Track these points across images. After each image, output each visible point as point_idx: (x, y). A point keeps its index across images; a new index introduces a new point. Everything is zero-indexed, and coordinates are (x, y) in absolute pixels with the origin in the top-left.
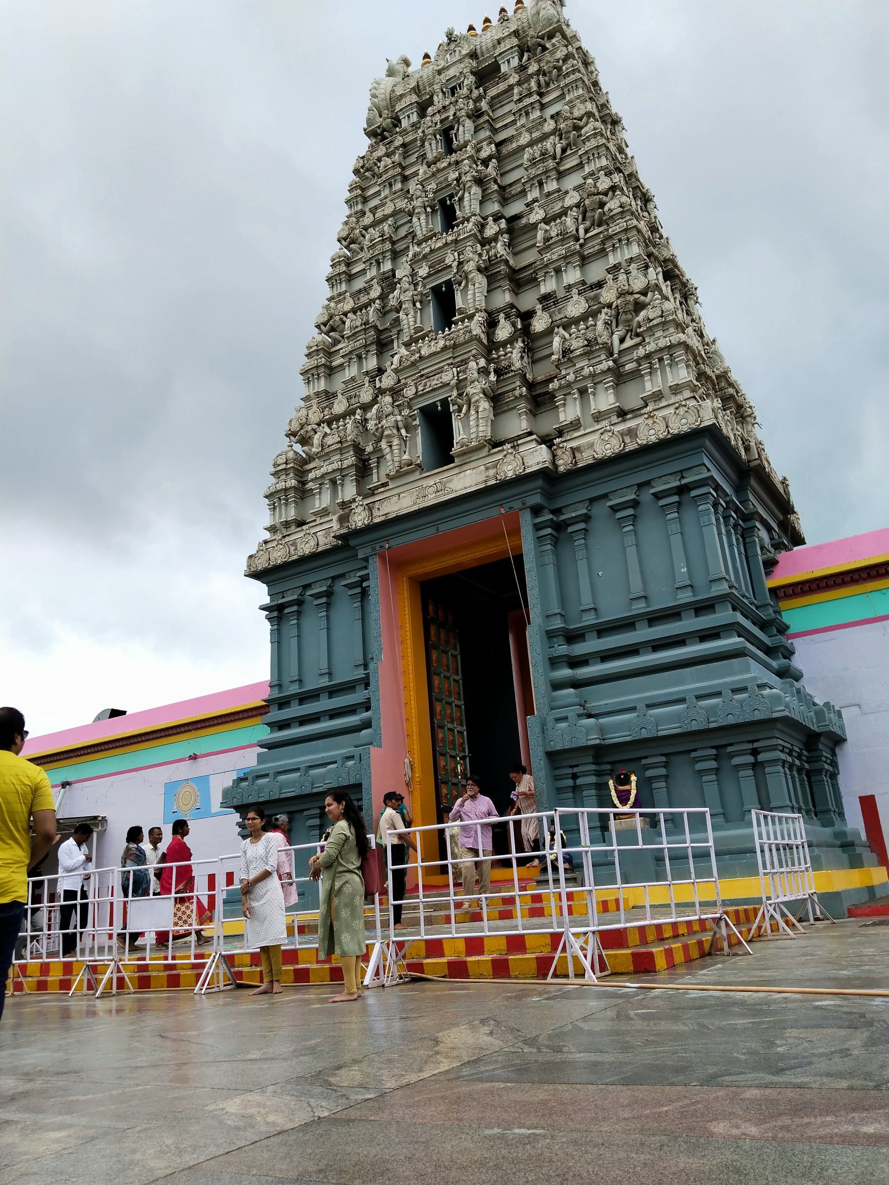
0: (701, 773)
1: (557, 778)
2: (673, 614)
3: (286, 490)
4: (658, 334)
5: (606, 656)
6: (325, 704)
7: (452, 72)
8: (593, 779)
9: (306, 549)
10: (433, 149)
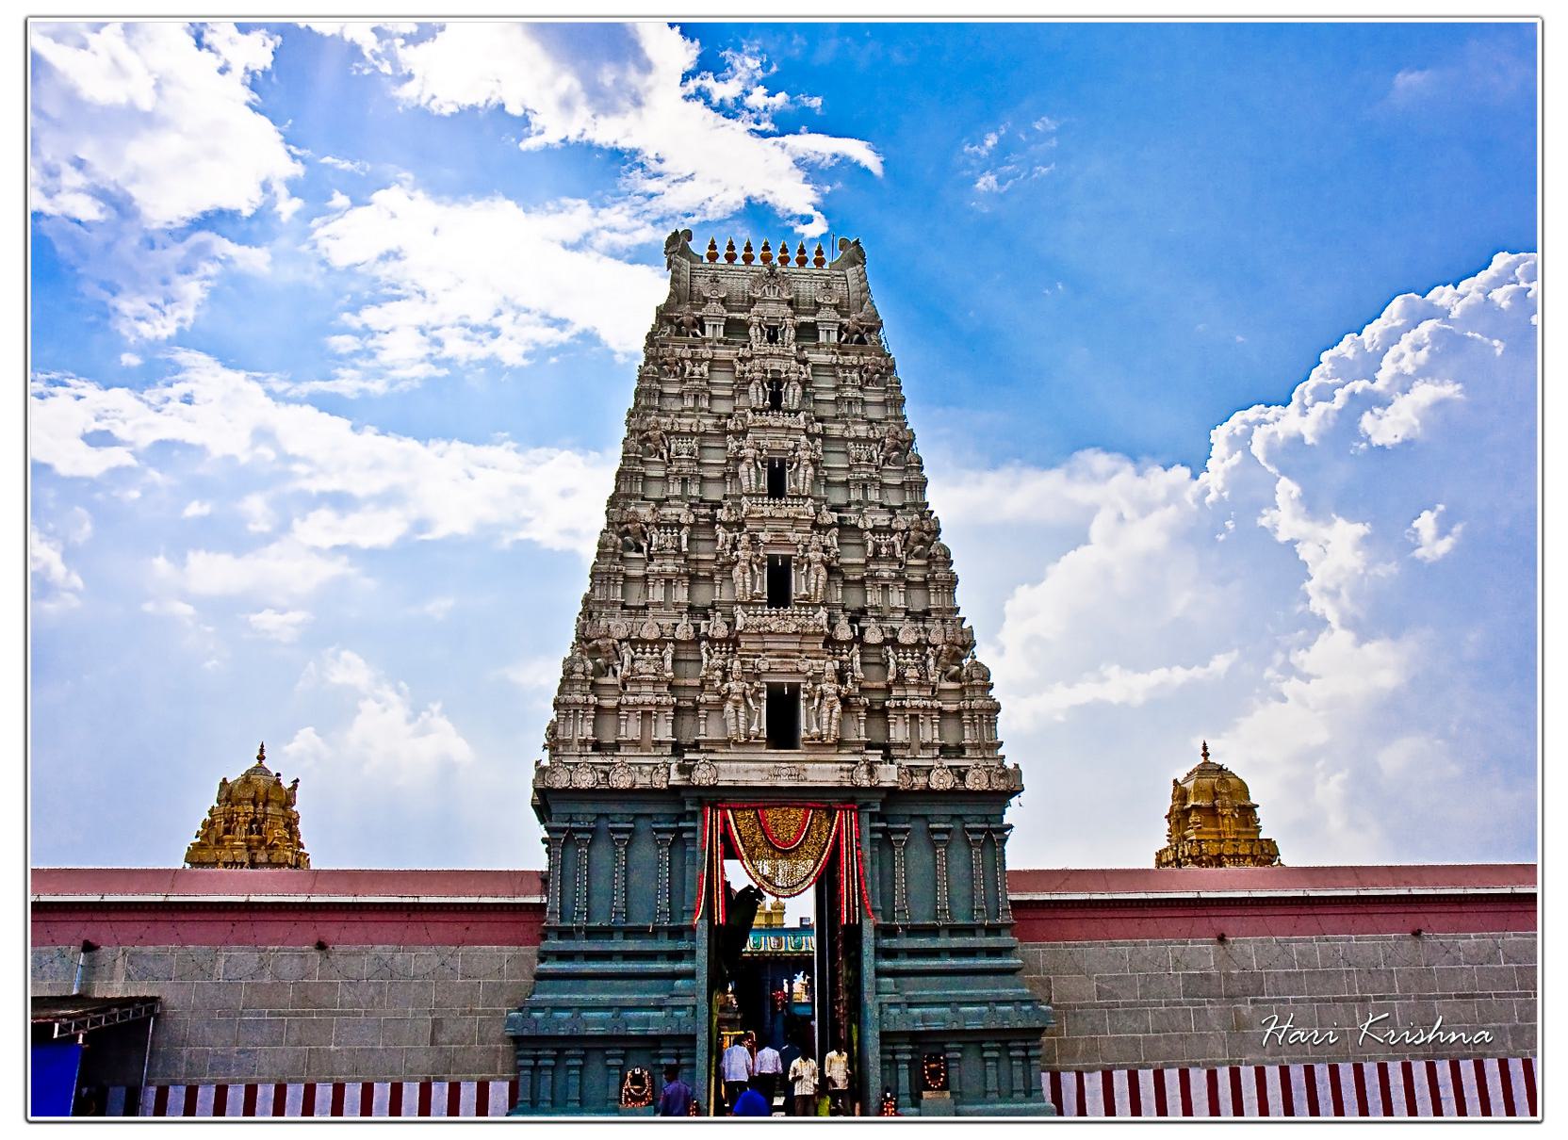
0: (985, 1060)
1: (882, 1052)
2: (970, 930)
3: (587, 705)
4: (978, 693)
5: (913, 953)
6: (618, 944)
7: (771, 310)
8: (908, 1057)
9: (621, 781)
10: (757, 396)
